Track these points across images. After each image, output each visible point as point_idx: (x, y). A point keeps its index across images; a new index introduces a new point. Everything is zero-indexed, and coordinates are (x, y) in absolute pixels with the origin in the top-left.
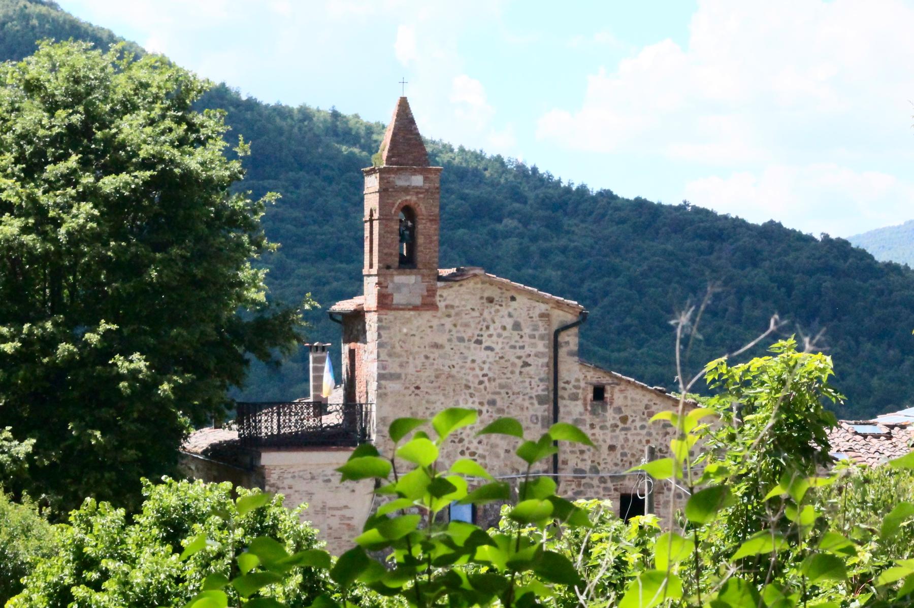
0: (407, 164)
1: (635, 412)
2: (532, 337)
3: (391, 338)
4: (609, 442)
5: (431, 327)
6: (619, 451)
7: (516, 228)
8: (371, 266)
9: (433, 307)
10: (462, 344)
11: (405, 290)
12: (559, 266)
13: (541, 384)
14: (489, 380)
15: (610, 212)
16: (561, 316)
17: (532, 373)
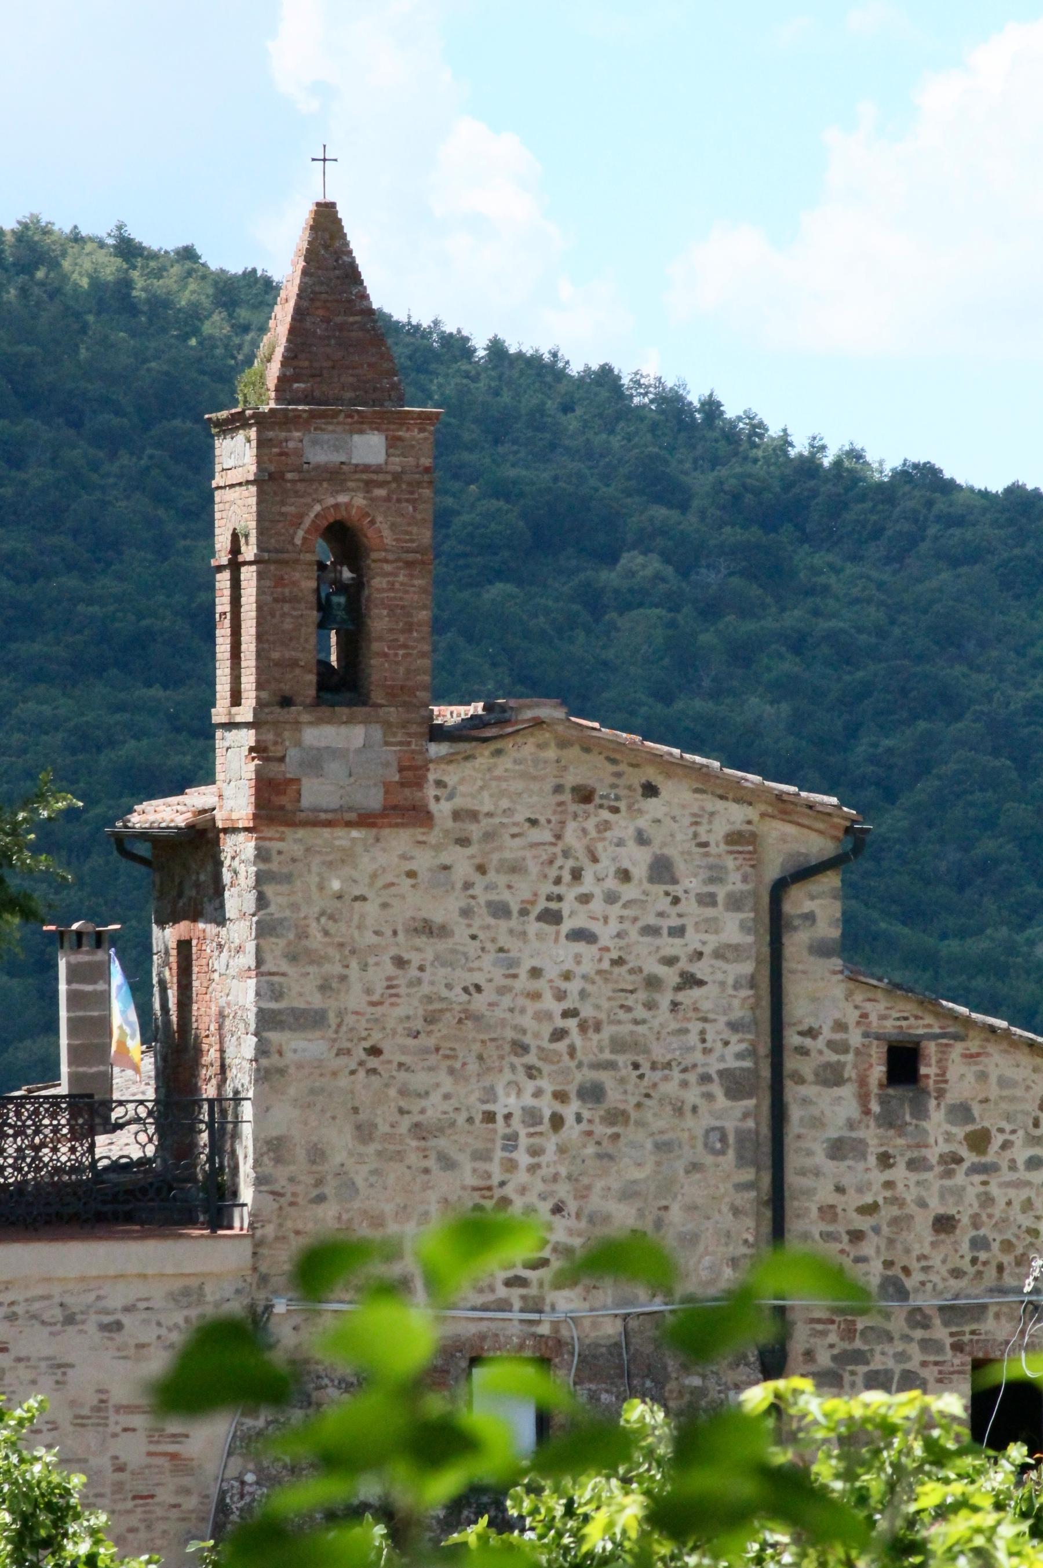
0: (338, 400)
1: (1008, 1118)
2: (708, 900)
3: (294, 907)
4: (936, 1207)
5: (411, 874)
6: (964, 1235)
7: (658, 577)
8: (236, 699)
9: (417, 815)
10: (503, 925)
11: (334, 768)
12: (781, 689)
13: (734, 1038)
14: (583, 1027)
15: (932, 530)
16: (788, 841)
17: (706, 1005)
